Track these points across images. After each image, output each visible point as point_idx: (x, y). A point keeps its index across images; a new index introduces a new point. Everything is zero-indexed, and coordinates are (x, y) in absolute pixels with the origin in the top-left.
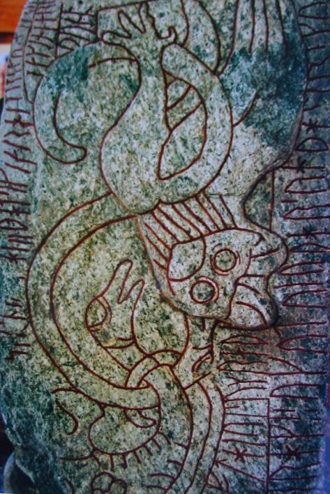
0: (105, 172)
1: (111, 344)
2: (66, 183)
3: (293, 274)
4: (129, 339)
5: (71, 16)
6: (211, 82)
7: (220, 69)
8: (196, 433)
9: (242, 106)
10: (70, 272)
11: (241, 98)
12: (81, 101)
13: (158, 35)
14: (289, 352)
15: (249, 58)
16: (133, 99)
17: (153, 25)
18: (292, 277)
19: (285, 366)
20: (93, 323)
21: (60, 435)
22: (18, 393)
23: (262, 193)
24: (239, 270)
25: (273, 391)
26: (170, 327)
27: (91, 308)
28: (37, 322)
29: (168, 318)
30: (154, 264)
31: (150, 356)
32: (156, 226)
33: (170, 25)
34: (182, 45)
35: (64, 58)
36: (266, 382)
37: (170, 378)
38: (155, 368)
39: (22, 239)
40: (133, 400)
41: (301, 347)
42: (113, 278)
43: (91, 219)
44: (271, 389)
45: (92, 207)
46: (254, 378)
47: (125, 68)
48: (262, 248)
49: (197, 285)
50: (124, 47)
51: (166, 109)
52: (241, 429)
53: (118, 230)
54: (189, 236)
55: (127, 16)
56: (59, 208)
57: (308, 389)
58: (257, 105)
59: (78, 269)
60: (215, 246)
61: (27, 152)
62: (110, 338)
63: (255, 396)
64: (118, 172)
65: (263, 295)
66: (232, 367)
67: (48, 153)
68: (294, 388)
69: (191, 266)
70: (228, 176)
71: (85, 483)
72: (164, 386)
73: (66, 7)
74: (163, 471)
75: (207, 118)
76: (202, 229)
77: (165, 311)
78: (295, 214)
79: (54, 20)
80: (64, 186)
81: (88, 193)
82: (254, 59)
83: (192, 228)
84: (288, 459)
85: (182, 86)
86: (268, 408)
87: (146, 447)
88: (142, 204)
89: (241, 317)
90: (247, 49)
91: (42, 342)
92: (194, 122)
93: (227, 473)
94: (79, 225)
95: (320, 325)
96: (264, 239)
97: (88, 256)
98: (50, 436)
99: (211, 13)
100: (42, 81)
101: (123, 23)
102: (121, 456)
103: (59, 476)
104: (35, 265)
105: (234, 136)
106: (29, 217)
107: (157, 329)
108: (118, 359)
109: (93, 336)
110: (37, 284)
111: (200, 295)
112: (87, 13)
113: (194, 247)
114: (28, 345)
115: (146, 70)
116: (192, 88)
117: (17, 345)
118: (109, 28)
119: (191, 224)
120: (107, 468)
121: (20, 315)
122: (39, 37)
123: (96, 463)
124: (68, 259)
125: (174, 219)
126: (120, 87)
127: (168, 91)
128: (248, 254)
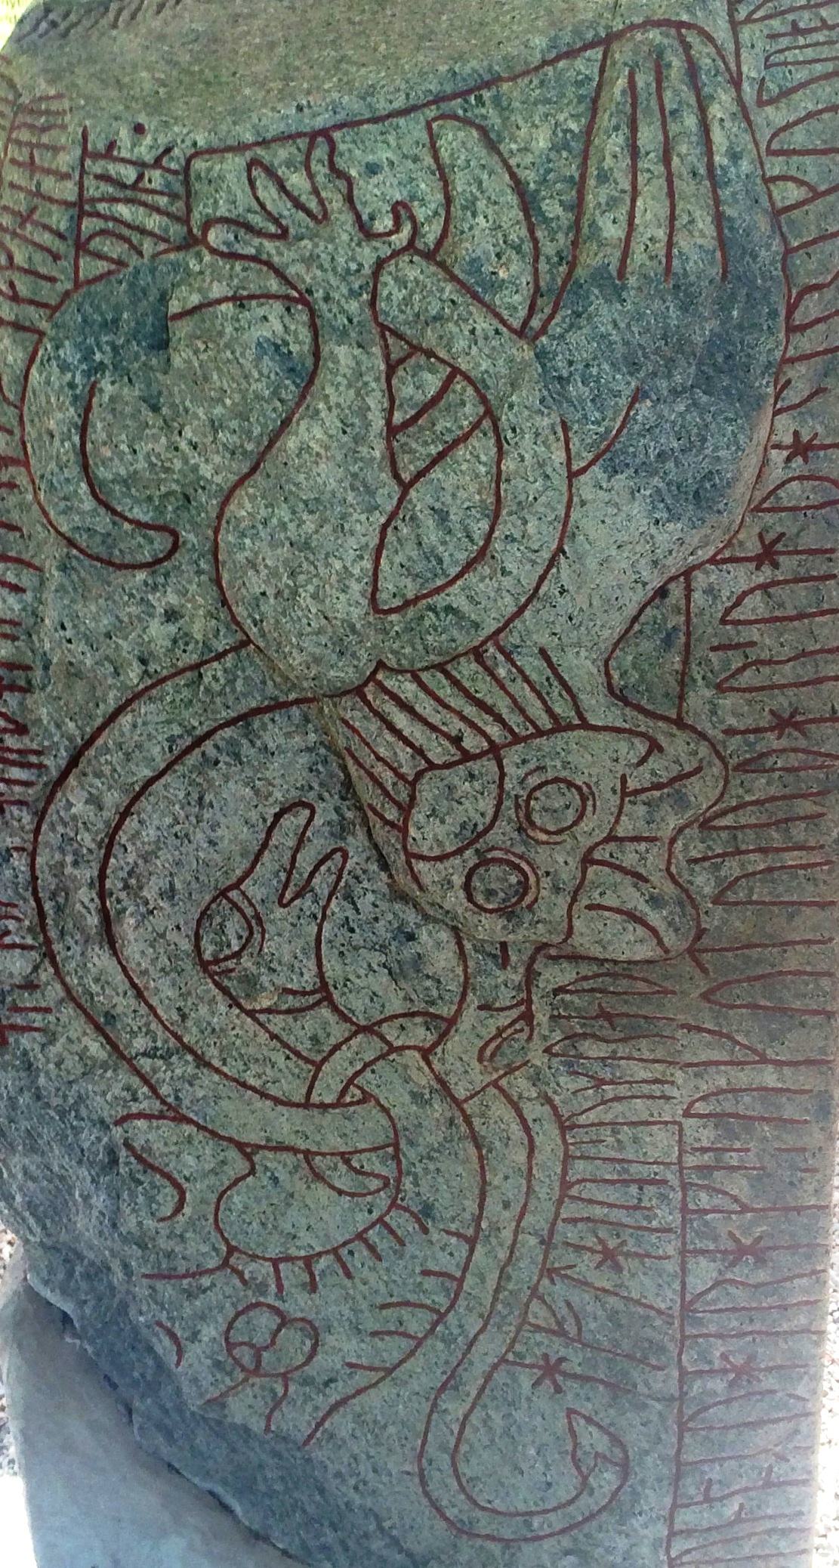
0: (228, 594)
1: (266, 1003)
3: (743, 827)
4: (312, 993)
7: (535, 323)
8: (493, 1205)
9: (597, 423)
10: (150, 834)
12: (155, 409)
13: (365, 231)
16: (298, 405)
17: (349, 199)
18: (740, 836)
20: (215, 955)
21: (140, 1224)
22: (25, 1124)
23: (655, 632)
24: (594, 827)
25: (691, 1104)
27: (210, 917)
28: (64, 953)
29: (411, 937)
30: (370, 814)
31: (368, 1029)
32: (374, 725)
34: (429, 256)
35: (99, 287)
36: (672, 1083)
37: (423, 1079)
38: (382, 1057)
39: (14, 756)
40: (330, 1133)
42: (265, 845)
43: (198, 707)
45: (200, 676)
47: (272, 322)
48: (653, 773)
49: (482, 870)
50: (269, 264)
51: (392, 431)
52: (611, 1195)
53: (273, 732)
55: (270, 172)
56: (110, 681)
61: (13, 536)
62: (263, 989)
63: (645, 1117)
64: (264, 594)
66: (581, 1049)
67: (71, 543)
68: (747, 1099)
69: (463, 826)
71: (210, 1332)
72: (407, 1098)
74: (412, 1298)
75: (501, 453)
76: (494, 731)
78: (748, 678)
79: (65, 176)
80: (120, 627)
82: (630, 295)
83: (468, 732)
84: (733, 1264)
85: (432, 371)
86: (680, 1141)
87: (366, 1241)
90: (613, 269)
91: (83, 1001)
93: (578, 1297)
94: (169, 722)
95: (815, 947)
96: (661, 749)
97: (196, 796)
98: (114, 1225)
99: (512, 162)
101: (260, 193)
102: (301, 1263)
103: (141, 1313)
104: (51, 816)
106: (29, 701)
109: (217, 984)
110: (62, 864)
111: (490, 894)
112: (157, 163)
114: (47, 1010)
116: (458, 378)
117: (16, 1009)
118: (223, 211)
119: (463, 718)
120: (264, 1293)
121: (18, 940)
122: (24, 219)
123: (237, 1282)
124: (143, 803)
125: (417, 708)
126: (261, 374)
127: (394, 382)
128: (618, 787)
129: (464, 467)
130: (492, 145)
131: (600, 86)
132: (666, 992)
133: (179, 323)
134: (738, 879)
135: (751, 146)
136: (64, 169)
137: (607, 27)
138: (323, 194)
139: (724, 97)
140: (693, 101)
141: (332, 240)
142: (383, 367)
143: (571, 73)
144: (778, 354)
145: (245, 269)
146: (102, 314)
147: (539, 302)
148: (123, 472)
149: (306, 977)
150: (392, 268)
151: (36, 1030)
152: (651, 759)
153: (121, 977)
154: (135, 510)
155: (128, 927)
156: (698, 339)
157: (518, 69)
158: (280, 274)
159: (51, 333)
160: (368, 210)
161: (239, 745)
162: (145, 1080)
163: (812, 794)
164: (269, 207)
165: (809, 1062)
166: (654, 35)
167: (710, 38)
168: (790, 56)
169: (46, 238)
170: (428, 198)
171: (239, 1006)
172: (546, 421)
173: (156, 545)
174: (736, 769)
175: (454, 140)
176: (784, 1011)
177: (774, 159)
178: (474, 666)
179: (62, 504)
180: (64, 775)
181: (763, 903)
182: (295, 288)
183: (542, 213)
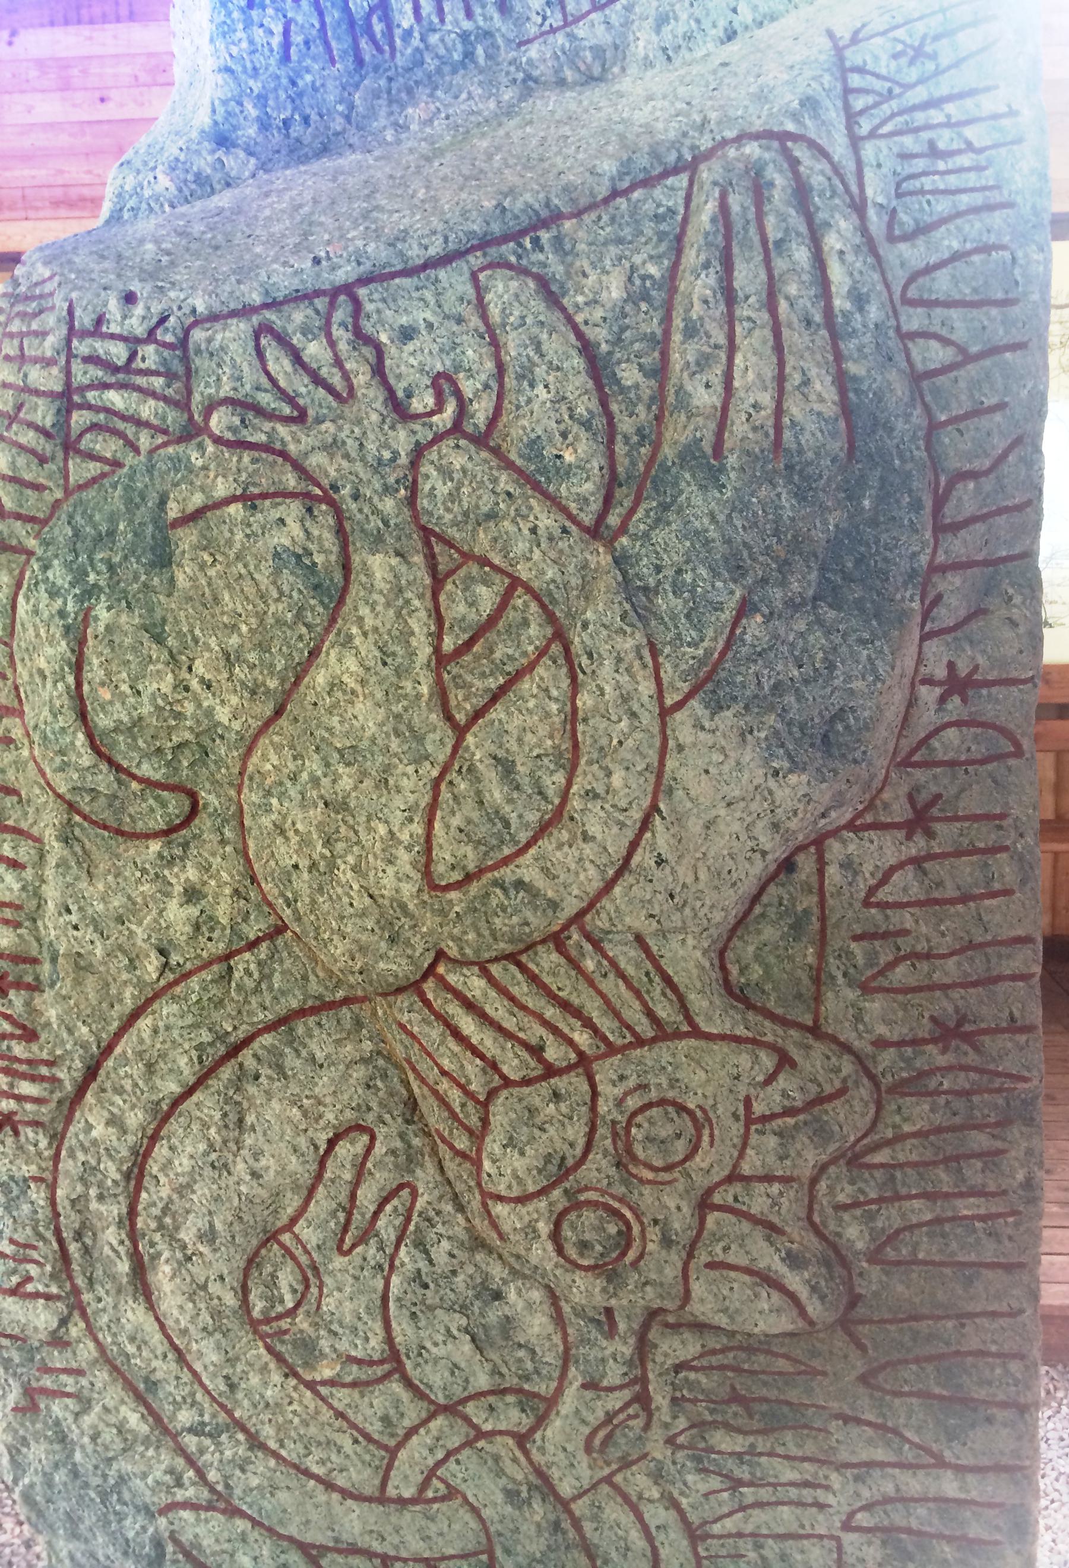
0: (256, 866)
1: (328, 1373)
2: (139, 900)
3: (901, 1166)
4: (381, 1362)
5: (101, 347)
6: (585, 566)
7: (613, 520)
9: (694, 644)
10: (183, 1164)
11: (688, 616)
12: (159, 639)
13: (399, 409)
14: (897, 1401)
15: (712, 474)
16: (327, 630)
17: (379, 370)
18: (898, 1174)
19: (888, 1444)
20: (265, 1311)
22: (63, 1505)
25: (851, 1515)
26: (508, 1323)
29: (498, 1296)
31: (451, 1409)
32: (435, 1032)
33: (439, 368)
34: (480, 440)
36: (827, 1488)
37: (519, 1473)
38: (468, 1444)
39: (24, 1068)
41: (937, 1390)
42: (319, 1177)
44: (846, 1509)
46: (790, 1475)
47: (289, 527)
48: (784, 1094)
49: (572, 1216)
50: (283, 454)
51: (441, 660)
53: (320, 1040)
54: (541, 1060)
55: (282, 340)
56: (125, 976)
57: (968, 1514)
58: (748, 638)
59: (206, 1154)
60: (626, 1094)
61: (10, 801)
62: (323, 1355)
63: (794, 1528)
64: (296, 866)
65: (799, 1236)
66: (712, 1442)
67: (72, 807)
68: (922, 1511)
69: (548, 1159)
70: (658, 874)
72: (499, 1497)
73: (84, 319)
75: (575, 686)
76: (582, 1038)
77: (487, 1277)
78: (901, 974)
79: (49, 363)
81: (212, 929)
83: (550, 1039)
85: (487, 583)
88: (382, 965)
89: (725, 1311)
90: (707, 447)
91: (118, 1363)
92: (531, 704)
95: (1003, 1322)
96: (793, 1064)
97: (233, 1117)
99: (579, 319)
100: (28, 574)
101: (271, 367)
104: (70, 1141)
105: (671, 743)
106: (37, 1001)
107: (467, 1331)
108: (350, 1413)
109: (269, 1349)
110: (85, 1196)
111: (584, 1246)
112: (151, 337)
113: (556, 1096)
114: (79, 1372)
115: (363, 531)
116: (520, 590)
117: (47, 1370)
118: (226, 390)
121: (41, 1288)
124: (175, 1126)
125: (489, 1010)
126: (281, 593)
127: (442, 598)
128: (741, 1111)
129: (531, 704)
130: (550, 293)
131: (685, 220)
132: (815, 1373)
133: (180, 532)
134: (898, 1232)
135: (880, 287)
136: (49, 354)
137: (693, 148)
138: (348, 366)
139: (843, 224)
140: (803, 229)
141: (359, 422)
142: (428, 581)
143: (649, 207)
144: (924, 559)
145: (254, 461)
146: (95, 527)
147: (618, 493)
148: (126, 719)
149: (373, 1343)
150: (434, 456)
151: (68, 1395)
152: (781, 1078)
153: (158, 1336)
154: (145, 766)
155: (162, 1277)
156: (819, 535)
157: (583, 202)
158: (298, 467)
159: (39, 552)
160: (403, 384)
161: (282, 1055)
162: (191, 1462)
163: (987, 1126)
164: (282, 384)
165: (999, 1468)
166: (752, 149)
167: (823, 153)
168: (927, 183)
169: (28, 438)
170: (475, 367)
171: (296, 1375)
172: (629, 644)
173: (171, 810)
174: (892, 1090)
175: (501, 290)
176: (967, 1402)
177: (911, 310)
178: (555, 957)
179: (58, 760)
180: (81, 1091)
181: (933, 1263)
182: (319, 486)
183: (618, 382)
